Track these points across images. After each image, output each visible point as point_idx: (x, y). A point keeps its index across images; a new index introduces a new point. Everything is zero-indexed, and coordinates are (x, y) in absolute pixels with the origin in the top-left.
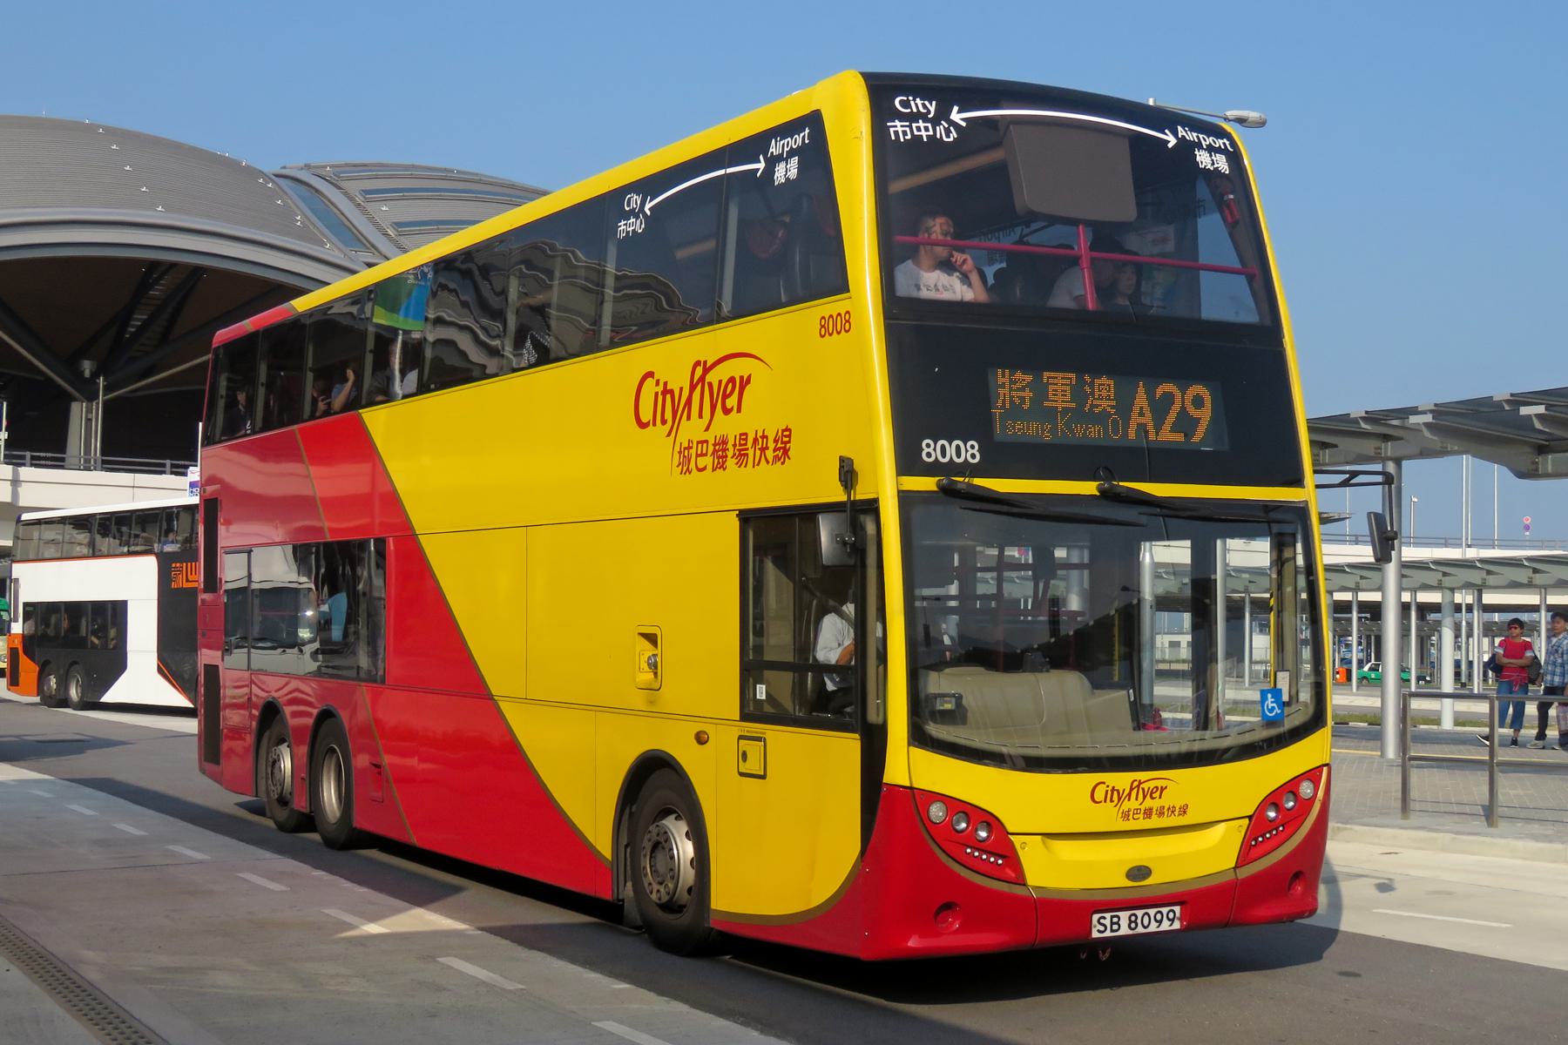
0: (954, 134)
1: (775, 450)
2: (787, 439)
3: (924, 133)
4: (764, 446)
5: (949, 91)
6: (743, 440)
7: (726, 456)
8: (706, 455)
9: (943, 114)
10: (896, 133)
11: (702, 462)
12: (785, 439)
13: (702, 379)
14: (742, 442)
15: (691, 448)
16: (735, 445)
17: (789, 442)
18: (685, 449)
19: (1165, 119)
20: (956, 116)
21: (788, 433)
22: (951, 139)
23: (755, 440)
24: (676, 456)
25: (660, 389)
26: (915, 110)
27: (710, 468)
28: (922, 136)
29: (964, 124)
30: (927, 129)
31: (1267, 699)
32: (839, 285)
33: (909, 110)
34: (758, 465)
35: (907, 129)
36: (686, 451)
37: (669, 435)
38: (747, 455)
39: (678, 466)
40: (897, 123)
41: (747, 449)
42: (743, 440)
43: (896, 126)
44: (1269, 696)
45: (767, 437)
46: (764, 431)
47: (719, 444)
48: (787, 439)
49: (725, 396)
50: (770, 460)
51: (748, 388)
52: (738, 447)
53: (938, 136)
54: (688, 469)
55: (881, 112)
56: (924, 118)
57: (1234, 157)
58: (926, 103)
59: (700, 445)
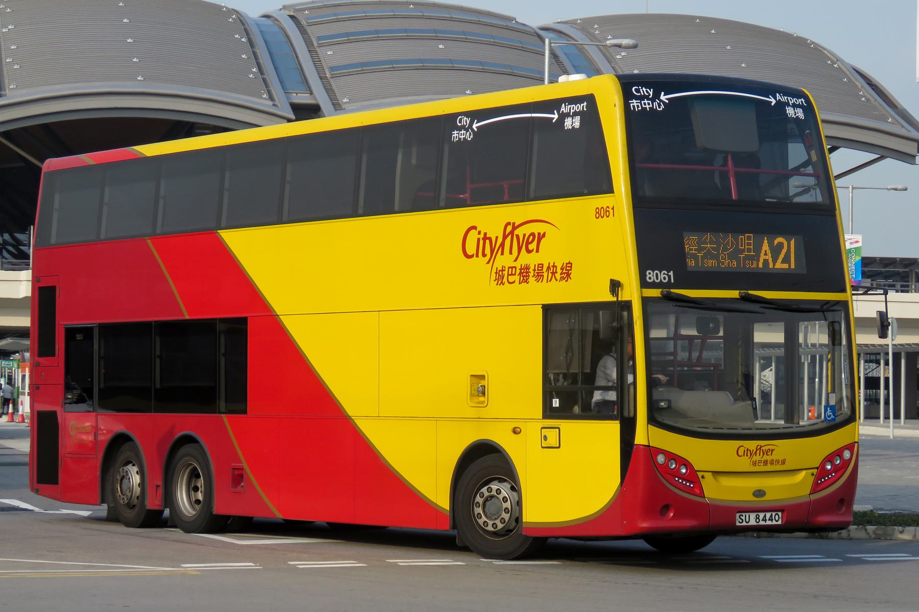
0: (662, 106)
1: (561, 274)
2: (570, 268)
3: (647, 106)
4: (554, 271)
5: (660, 83)
6: (540, 267)
7: (529, 276)
8: (515, 274)
9: (656, 96)
10: (634, 106)
11: (511, 279)
12: (568, 268)
13: (512, 232)
14: (539, 269)
15: (505, 270)
16: (534, 270)
17: (571, 270)
18: (499, 271)
19: (770, 90)
20: (663, 97)
21: (570, 265)
22: (661, 109)
23: (549, 268)
24: (494, 275)
25: (482, 236)
26: (643, 94)
27: (517, 281)
28: (646, 107)
29: (667, 102)
30: (649, 104)
31: (827, 410)
32: (607, 188)
33: (640, 94)
34: (550, 281)
35: (639, 104)
36: (501, 272)
37: (488, 262)
38: (543, 275)
39: (495, 281)
40: (634, 101)
41: (543, 273)
42: (540, 267)
43: (633, 103)
44: (829, 409)
45: (556, 267)
46: (554, 264)
47: (523, 269)
48: (570, 268)
49: (528, 243)
50: (558, 278)
51: (543, 241)
52: (536, 271)
53: (655, 108)
54: (502, 282)
55: (627, 96)
56: (647, 97)
57: (808, 109)
58: (648, 90)
59: (510, 270)
